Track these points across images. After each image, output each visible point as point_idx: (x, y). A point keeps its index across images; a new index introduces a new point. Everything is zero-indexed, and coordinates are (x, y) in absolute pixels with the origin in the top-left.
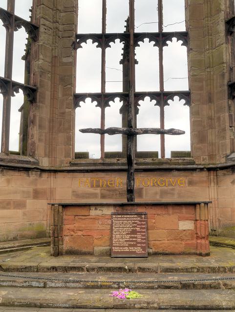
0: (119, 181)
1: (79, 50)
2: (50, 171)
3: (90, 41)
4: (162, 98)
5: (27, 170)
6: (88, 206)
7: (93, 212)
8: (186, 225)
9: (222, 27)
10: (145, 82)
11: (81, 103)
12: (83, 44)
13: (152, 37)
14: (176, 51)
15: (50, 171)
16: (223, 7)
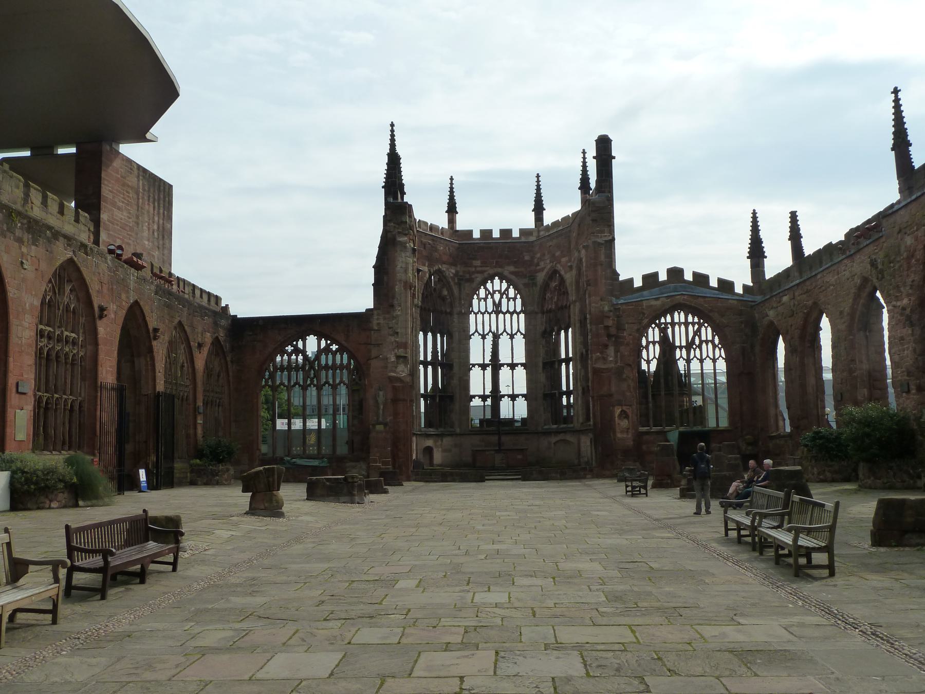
0: (494, 439)
1: (471, 371)
2: (461, 435)
3: (477, 366)
4: (513, 397)
5: (451, 435)
6: (485, 450)
7: (487, 453)
8: (519, 457)
9: (541, 365)
10: (504, 389)
11: (473, 399)
12: (473, 368)
13: (508, 365)
14: (521, 373)
15: (461, 435)
16: (541, 355)
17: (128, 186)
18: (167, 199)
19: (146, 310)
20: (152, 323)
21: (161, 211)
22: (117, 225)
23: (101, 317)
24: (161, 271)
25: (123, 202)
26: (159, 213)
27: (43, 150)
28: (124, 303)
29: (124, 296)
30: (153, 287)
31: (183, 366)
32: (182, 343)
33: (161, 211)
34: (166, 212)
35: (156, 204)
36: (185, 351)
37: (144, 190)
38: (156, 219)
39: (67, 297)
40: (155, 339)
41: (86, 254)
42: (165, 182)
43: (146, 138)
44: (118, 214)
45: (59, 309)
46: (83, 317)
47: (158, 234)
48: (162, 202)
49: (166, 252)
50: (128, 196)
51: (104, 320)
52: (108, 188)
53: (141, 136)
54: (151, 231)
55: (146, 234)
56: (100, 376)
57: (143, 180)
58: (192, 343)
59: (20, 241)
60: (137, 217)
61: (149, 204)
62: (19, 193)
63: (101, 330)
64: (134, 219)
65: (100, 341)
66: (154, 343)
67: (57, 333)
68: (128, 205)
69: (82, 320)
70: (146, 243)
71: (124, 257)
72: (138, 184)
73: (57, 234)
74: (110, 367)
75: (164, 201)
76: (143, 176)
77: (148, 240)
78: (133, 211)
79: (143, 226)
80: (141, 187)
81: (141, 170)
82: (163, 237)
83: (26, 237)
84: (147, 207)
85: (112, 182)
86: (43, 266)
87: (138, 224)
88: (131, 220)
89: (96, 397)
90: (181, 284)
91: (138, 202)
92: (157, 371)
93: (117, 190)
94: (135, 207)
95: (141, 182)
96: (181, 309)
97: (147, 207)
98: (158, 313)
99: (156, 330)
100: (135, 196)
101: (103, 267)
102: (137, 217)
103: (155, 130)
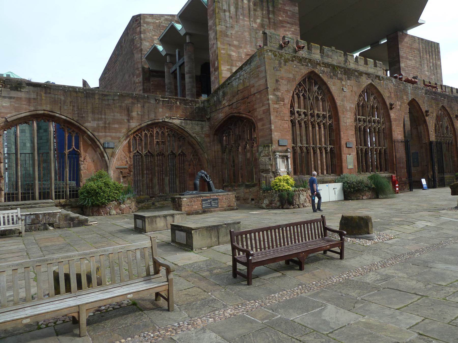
17: (414, 48)
18: (437, 50)
19: (420, 102)
20: (424, 108)
21: (434, 56)
22: (410, 67)
23: (391, 109)
24: (430, 83)
25: (412, 56)
26: (432, 58)
27: (375, 44)
28: (405, 101)
29: (405, 97)
30: (424, 91)
31: (447, 128)
32: (446, 117)
33: (434, 56)
34: (437, 57)
35: (431, 54)
36: (448, 120)
37: (423, 48)
38: (431, 61)
39: (372, 101)
40: (427, 116)
41: (380, 80)
42: (434, 43)
43: (418, 23)
44: (409, 63)
45: (368, 108)
46: (382, 110)
47: (433, 68)
48: (434, 52)
49: (439, 75)
50: (415, 53)
51: (394, 110)
52: (403, 52)
53: (415, 23)
54: (429, 67)
55: (426, 69)
56: (394, 136)
57: (422, 44)
58: (451, 116)
59: (341, 79)
60: (421, 62)
61: (426, 55)
62: (342, 59)
63: (393, 115)
64: (419, 63)
65: (392, 120)
66: (427, 118)
67: (368, 119)
68: (415, 57)
69: (382, 111)
70: (427, 73)
71: (403, 79)
72: (419, 47)
73: (361, 74)
74: (399, 131)
75: (435, 51)
76: (422, 42)
77: (428, 72)
78: (418, 59)
79: (424, 66)
80: (421, 47)
81: (420, 39)
82: (436, 69)
83: (344, 77)
84: (425, 56)
85: (405, 48)
86: (355, 89)
87: (421, 65)
88: (417, 64)
89: (393, 146)
90: (444, 88)
91: (420, 55)
92: (430, 131)
93: (408, 52)
94: (419, 57)
95: (421, 45)
96: (443, 100)
97: (425, 56)
98: (428, 103)
99: (427, 112)
100: (418, 53)
101: (391, 85)
102: (421, 62)
103: (423, 18)
